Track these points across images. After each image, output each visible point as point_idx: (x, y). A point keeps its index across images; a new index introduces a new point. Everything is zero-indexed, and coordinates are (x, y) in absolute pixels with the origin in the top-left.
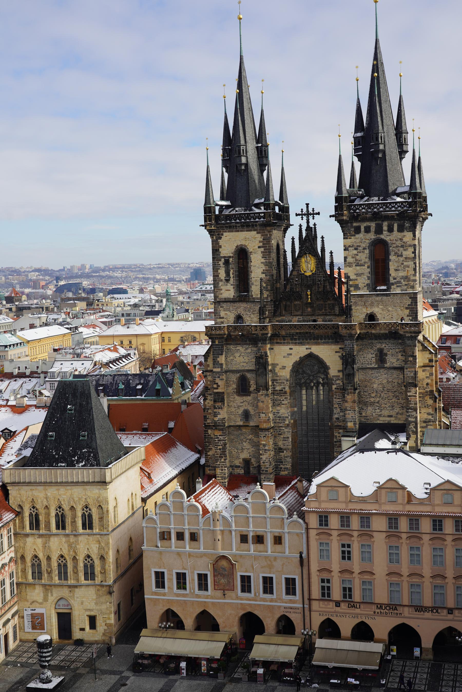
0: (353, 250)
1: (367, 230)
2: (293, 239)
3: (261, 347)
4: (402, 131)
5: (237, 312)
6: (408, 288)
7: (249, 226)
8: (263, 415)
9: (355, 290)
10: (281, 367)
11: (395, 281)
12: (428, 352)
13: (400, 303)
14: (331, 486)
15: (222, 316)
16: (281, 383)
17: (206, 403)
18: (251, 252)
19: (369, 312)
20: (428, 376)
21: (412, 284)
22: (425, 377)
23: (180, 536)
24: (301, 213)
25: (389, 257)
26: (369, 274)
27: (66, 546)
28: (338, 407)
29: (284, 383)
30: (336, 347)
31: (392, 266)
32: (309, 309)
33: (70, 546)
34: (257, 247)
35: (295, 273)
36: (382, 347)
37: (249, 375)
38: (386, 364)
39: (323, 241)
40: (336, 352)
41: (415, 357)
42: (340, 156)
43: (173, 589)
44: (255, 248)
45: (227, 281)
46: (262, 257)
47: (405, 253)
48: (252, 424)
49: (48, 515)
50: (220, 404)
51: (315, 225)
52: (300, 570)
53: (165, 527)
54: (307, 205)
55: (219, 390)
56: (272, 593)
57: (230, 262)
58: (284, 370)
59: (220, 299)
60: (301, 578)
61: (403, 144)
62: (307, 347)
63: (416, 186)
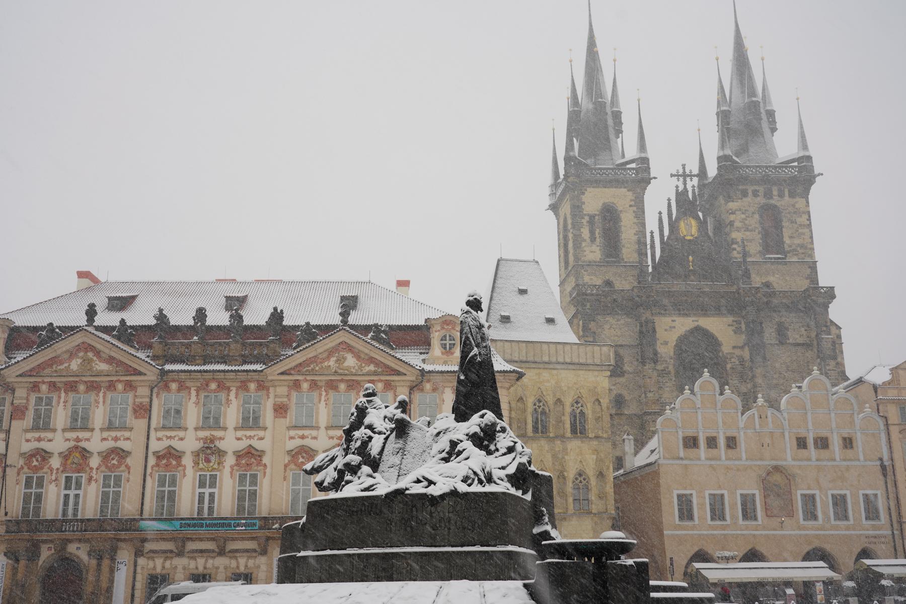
1: (755, 194)
2: (669, 200)
23: (712, 442)
27: (549, 457)
30: (730, 319)
31: (786, 233)
33: (554, 456)
37: (621, 351)
43: (706, 519)
47: (799, 220)
49: (525, 410)
52: (882, 483)
53: (690, 433)
54: (684, 166)
56: (846, 518)
60: (884, 493)
62: (694, 319)
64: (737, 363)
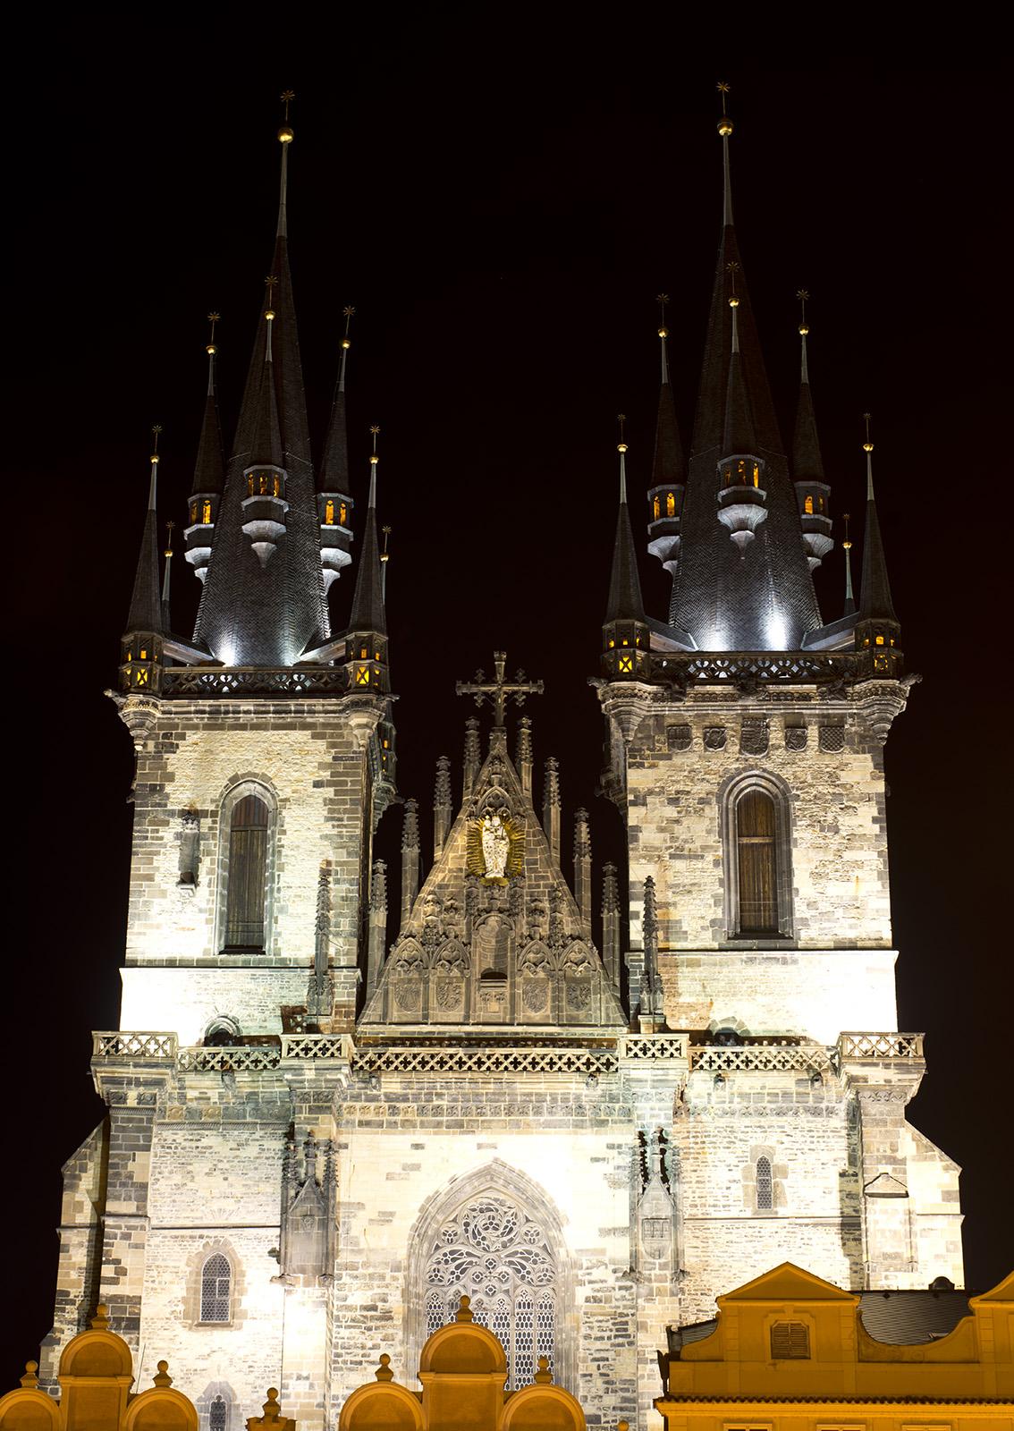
1: (715, 739)
8: (302, 1387)
10: (375, 1216)
11: (813, 912)
16: (371, 1276)
25: (788, 833)
26: (722, 885)
28: (596, 1373)
29: (383, 1277)
30: (594, 1141)
31: (803, 860)
32: (494, 1006)
36: (767, 1143)
40: (596, 1160)
46: (328, 819)
47: (846, 822)
55: (123, 1289)
58: (387, 1227)
62: (482, 1137)
64: (611, 1280)
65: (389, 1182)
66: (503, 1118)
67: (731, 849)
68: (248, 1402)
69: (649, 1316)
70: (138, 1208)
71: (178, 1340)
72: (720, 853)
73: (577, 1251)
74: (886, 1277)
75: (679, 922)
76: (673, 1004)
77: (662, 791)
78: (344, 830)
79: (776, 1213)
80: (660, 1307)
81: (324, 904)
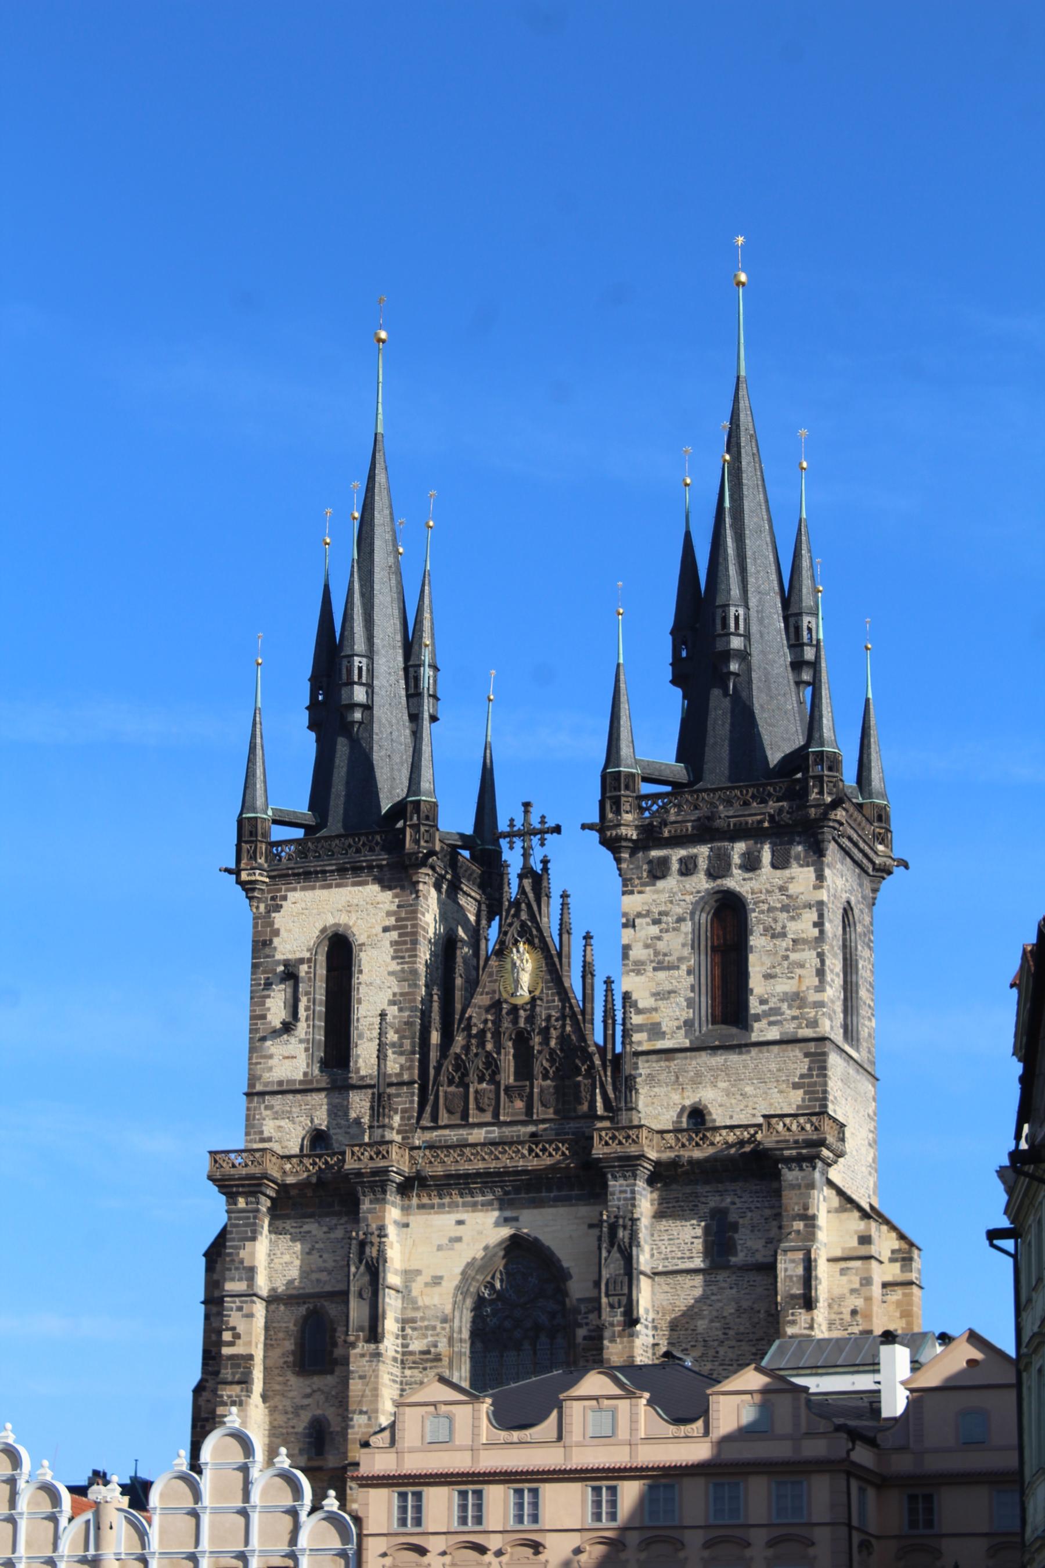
0: (648, 924)
3: (370, 1211)
4: (800, 608)
5: (312, 1121)
6: (800, 1027)
7: (362, 868)
9: (650, 1040)
10: (429, 1280)
11: (765, 1007)
12: (856, 1214)
13: (779, 1070)
14: (434, 1404)
15: (266, 1134)
16: (427, 1328)
17: (201, 1401)
18: (363, 944)
19: (688, 1103)
20: (857, 1286)
21: (812, 1015)
22: (846, 1291)
24: (508, 829)
25: (746, 941)
26: (693, 990)
29: (434, 1328)
31: (756, 966)
34: (379, 929)
35: (481, 999)
36: (723, 1205)
37: (332, 1309)
38: (735, 1254)
39: (564, 906)
40: (591, 1226)
41: (810, 1220)
42: (618, 665)
44: (374, 931)
45: (287, 1028)
46: (393, 958)
48: (332, 1461)
50: (237, 1388)
51: (545, 862)
54: (527, 805)
57: (302, 974)
58: (437, 1289)
59: (266, 1084)
61: (802, 645)
63: (821, 736)
65: (440, 1253)
66: (523, 1196)
67: (703, 957)
68: (338, 1429)
69: (612, 1354)
70: (248, 1286)
71: (289, 1383)
72: (692, 962)
73: (579, 1300)
74: (793, 1314)
75: (659, 1024)
76: (652, 1094)
77: (648, 913)
78: (406, 966)
79: (729, 1261)
80: (620, 1346)
81: (381, 1034)
